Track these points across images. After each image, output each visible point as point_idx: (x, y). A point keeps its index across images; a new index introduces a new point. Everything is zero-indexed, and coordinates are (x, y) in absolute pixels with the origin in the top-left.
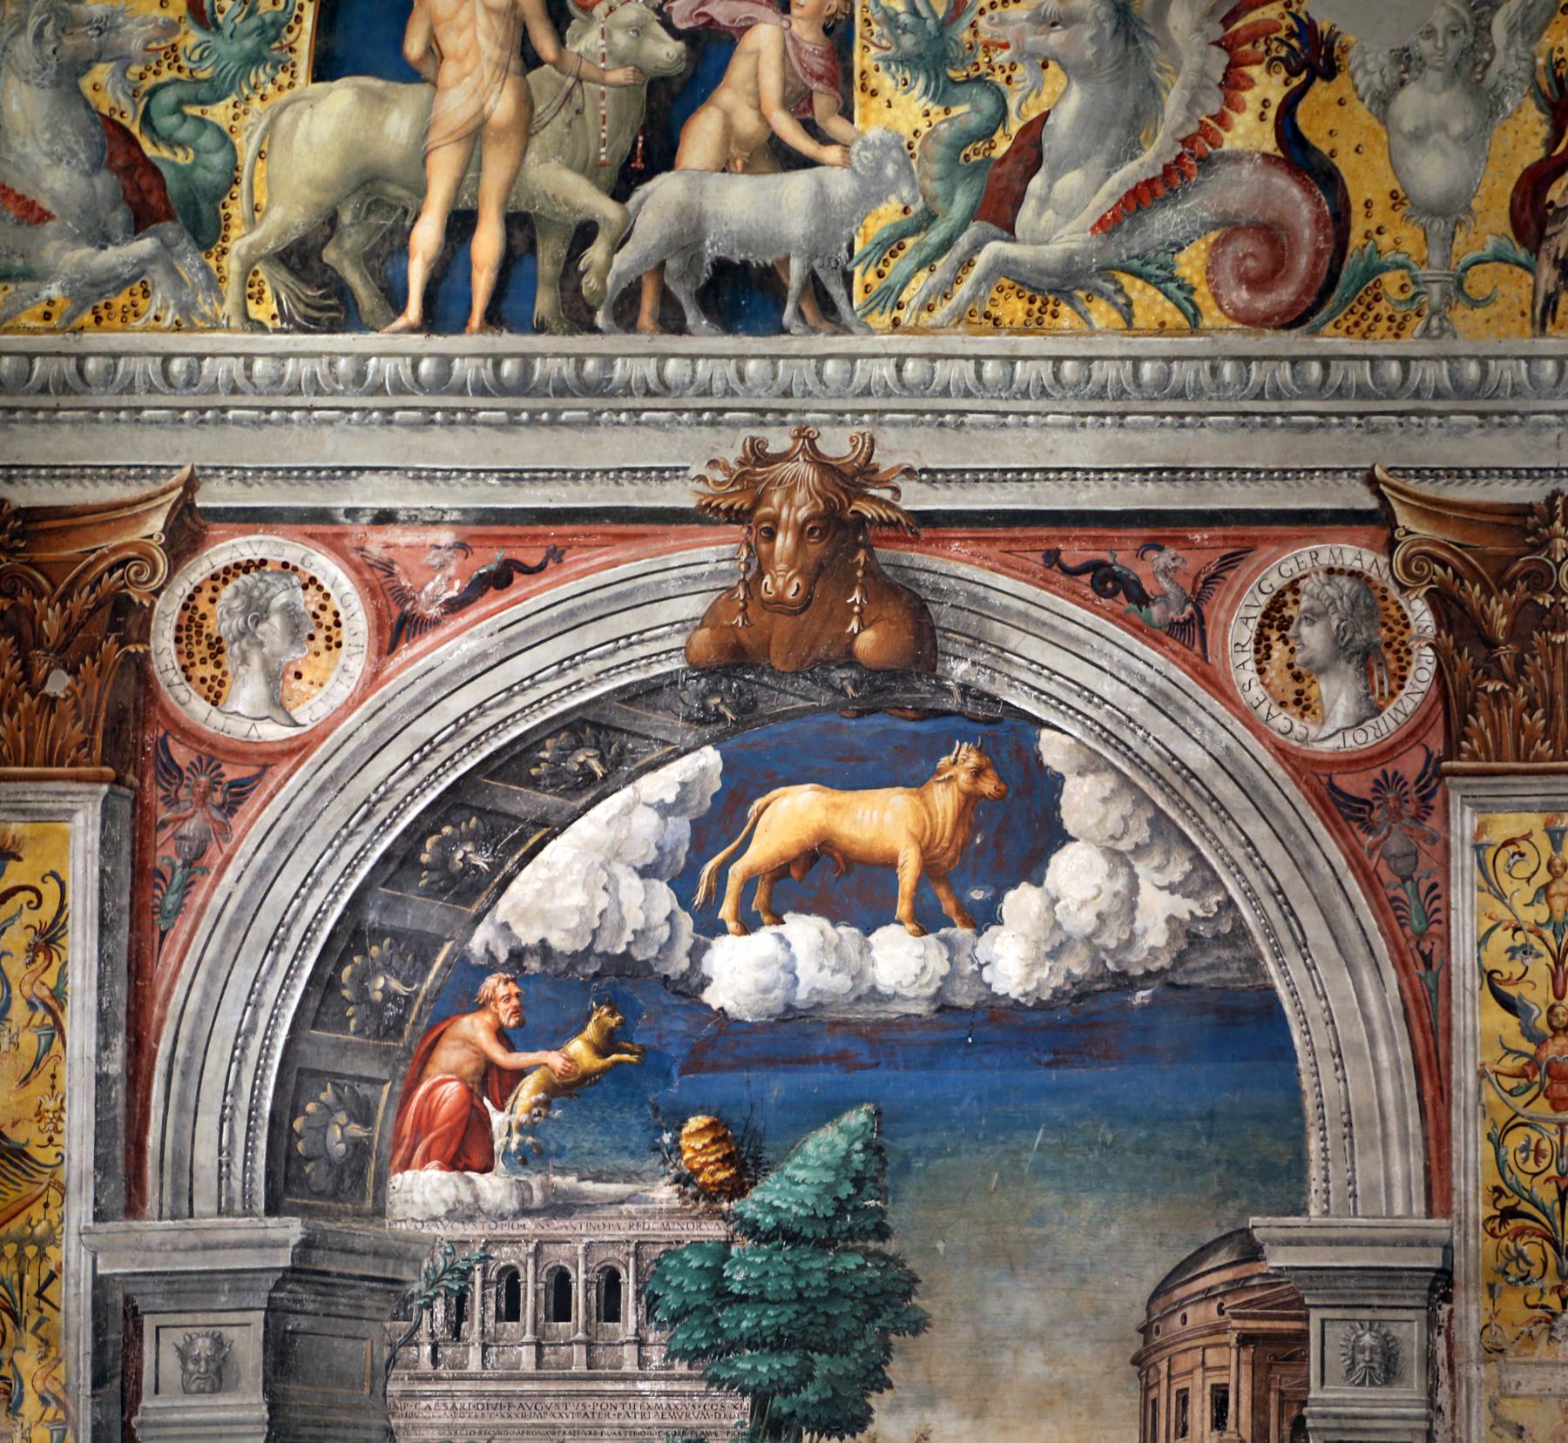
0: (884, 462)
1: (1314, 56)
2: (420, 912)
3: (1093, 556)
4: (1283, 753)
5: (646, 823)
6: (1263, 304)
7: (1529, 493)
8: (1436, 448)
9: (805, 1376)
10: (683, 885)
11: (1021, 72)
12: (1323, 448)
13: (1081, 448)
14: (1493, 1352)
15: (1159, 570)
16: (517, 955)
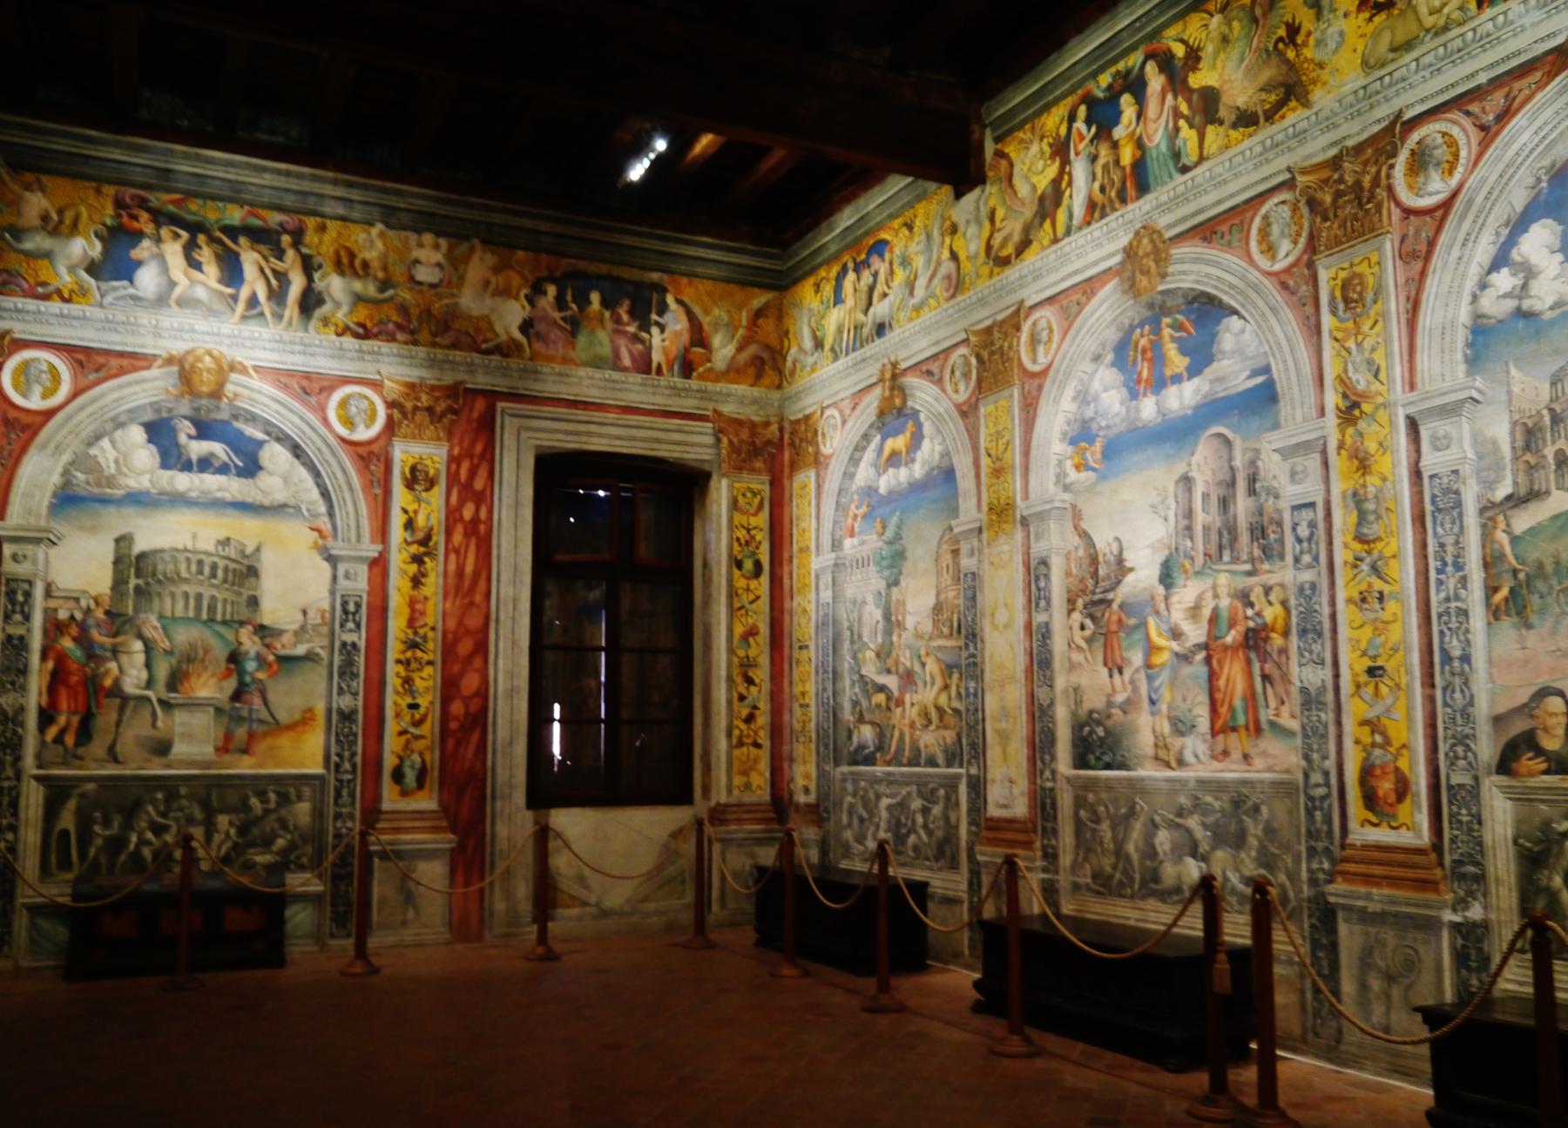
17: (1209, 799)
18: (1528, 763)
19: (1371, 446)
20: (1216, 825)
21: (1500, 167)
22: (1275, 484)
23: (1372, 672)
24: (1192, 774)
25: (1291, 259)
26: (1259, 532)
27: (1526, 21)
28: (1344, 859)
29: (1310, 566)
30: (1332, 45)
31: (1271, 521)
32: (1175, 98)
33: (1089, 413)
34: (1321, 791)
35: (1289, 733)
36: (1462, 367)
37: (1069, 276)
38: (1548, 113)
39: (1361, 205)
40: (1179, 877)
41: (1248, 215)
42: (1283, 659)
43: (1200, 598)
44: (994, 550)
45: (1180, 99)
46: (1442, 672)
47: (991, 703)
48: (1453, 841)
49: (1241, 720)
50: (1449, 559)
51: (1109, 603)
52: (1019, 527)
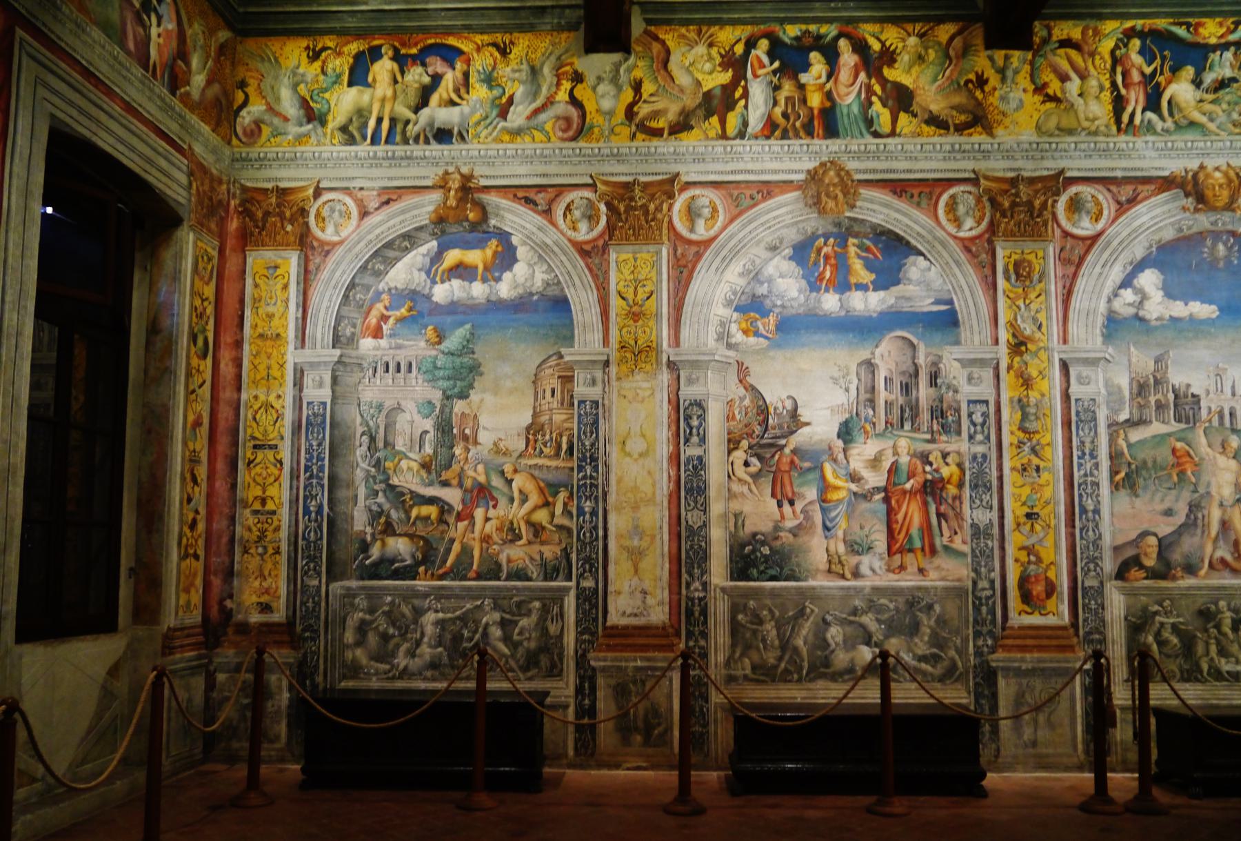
0: (475, 174)
1: (578, 78)
2: (368, 279)
3: (525, 195)
4: (570, 240)
5: (420, 258)
6: (566, 135)
7: (630, 179)
8: (607, 168)
9: (455, 386)
10: (428, 273)
11: (509, 83)
12: (582, 169)
13: (523, 170)
14: (619, 379)
15: (541, 198)
16: (390, 290)
17: (883, 601)
18: (1134, 573)
19: (1034, 373)
20: (892, 619)
21: (1128, 230)
22: (955, 382)
23: (1029, 516)
24: (868, 583)
25: (974, 233)
26: (938, 412)
27: (1147, 153)
28: (1004, 636)
29: (981, 443)
30: (1013, 105)
31: (950, 407)
32: (869, 77)
33: (762, 290)
34: (989, 593)
35: (964, 555)
36: (1099, 340)
37: (741, 172)
38: (1158, 211)
39: (1031, 215)
40: (852, 660)
41: (938, 191)
42: (957, 503)
43: (881, 453)
44: (626, 384)
45: (873, 81)
46: (1081, 518)
47: (616, 523)
48: (1084, 621)
49: (918, 544)
50: (1087, 451)
51: (782, 448)
52: (664, 368)
